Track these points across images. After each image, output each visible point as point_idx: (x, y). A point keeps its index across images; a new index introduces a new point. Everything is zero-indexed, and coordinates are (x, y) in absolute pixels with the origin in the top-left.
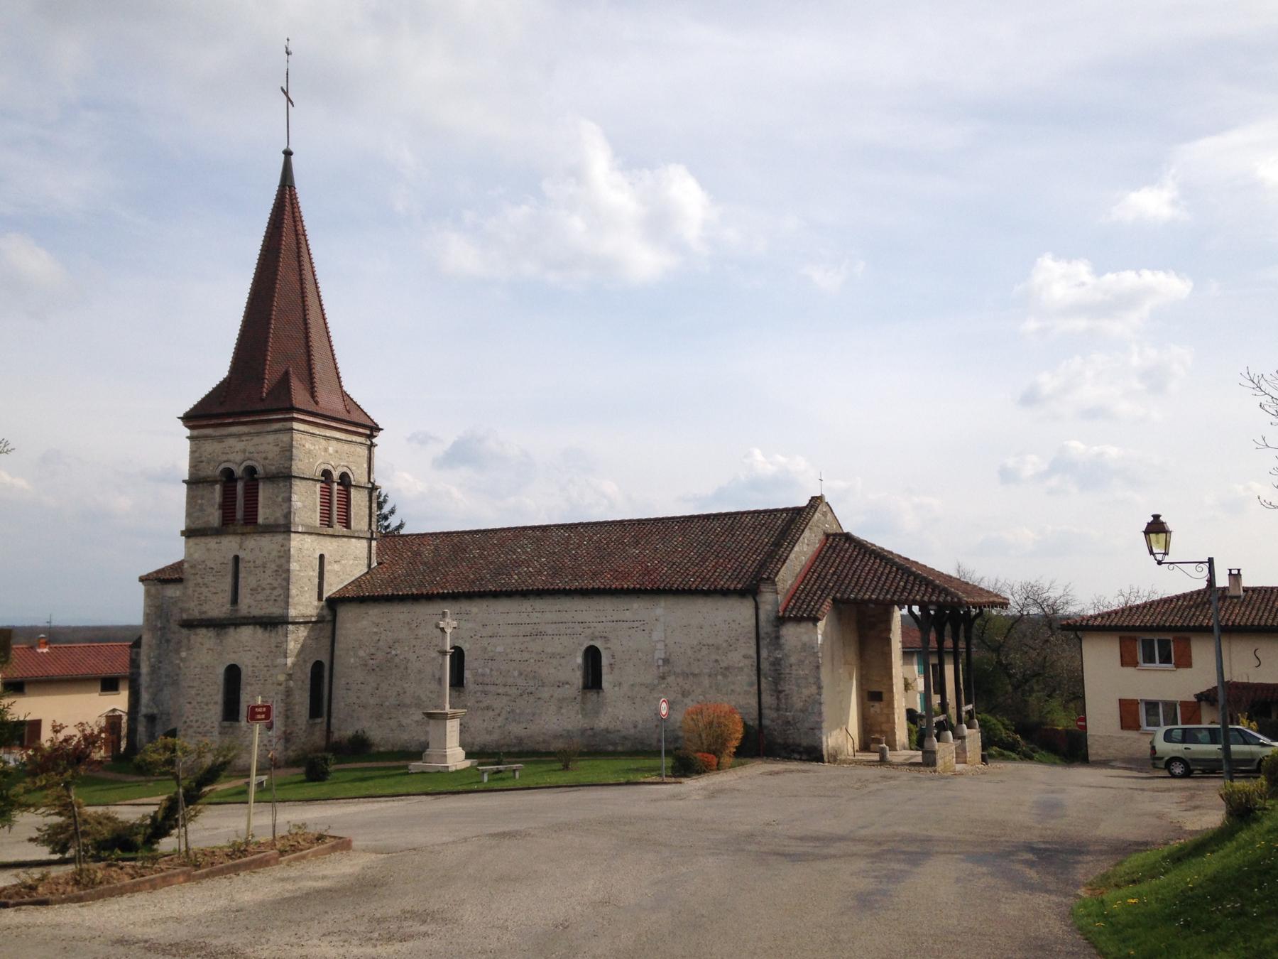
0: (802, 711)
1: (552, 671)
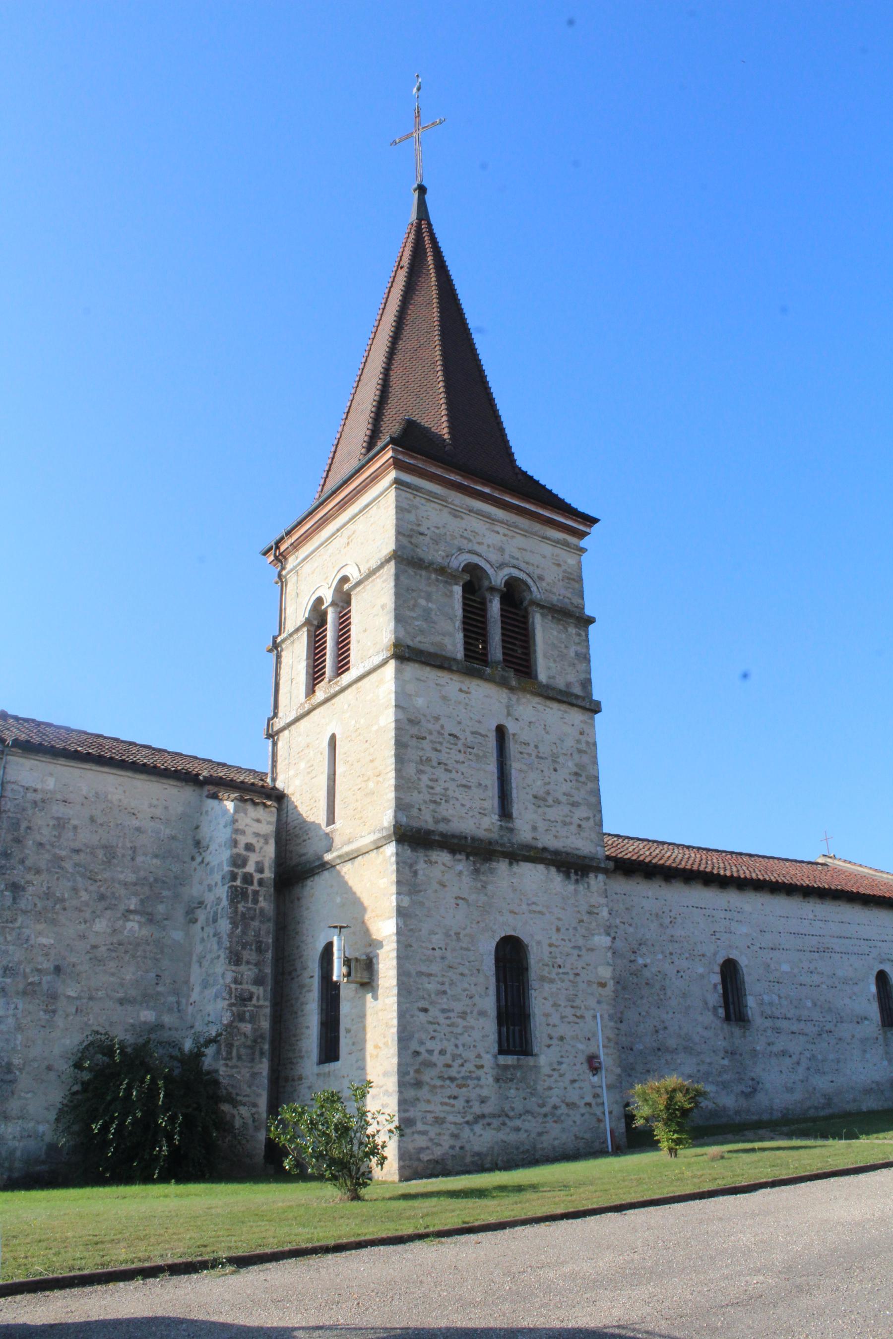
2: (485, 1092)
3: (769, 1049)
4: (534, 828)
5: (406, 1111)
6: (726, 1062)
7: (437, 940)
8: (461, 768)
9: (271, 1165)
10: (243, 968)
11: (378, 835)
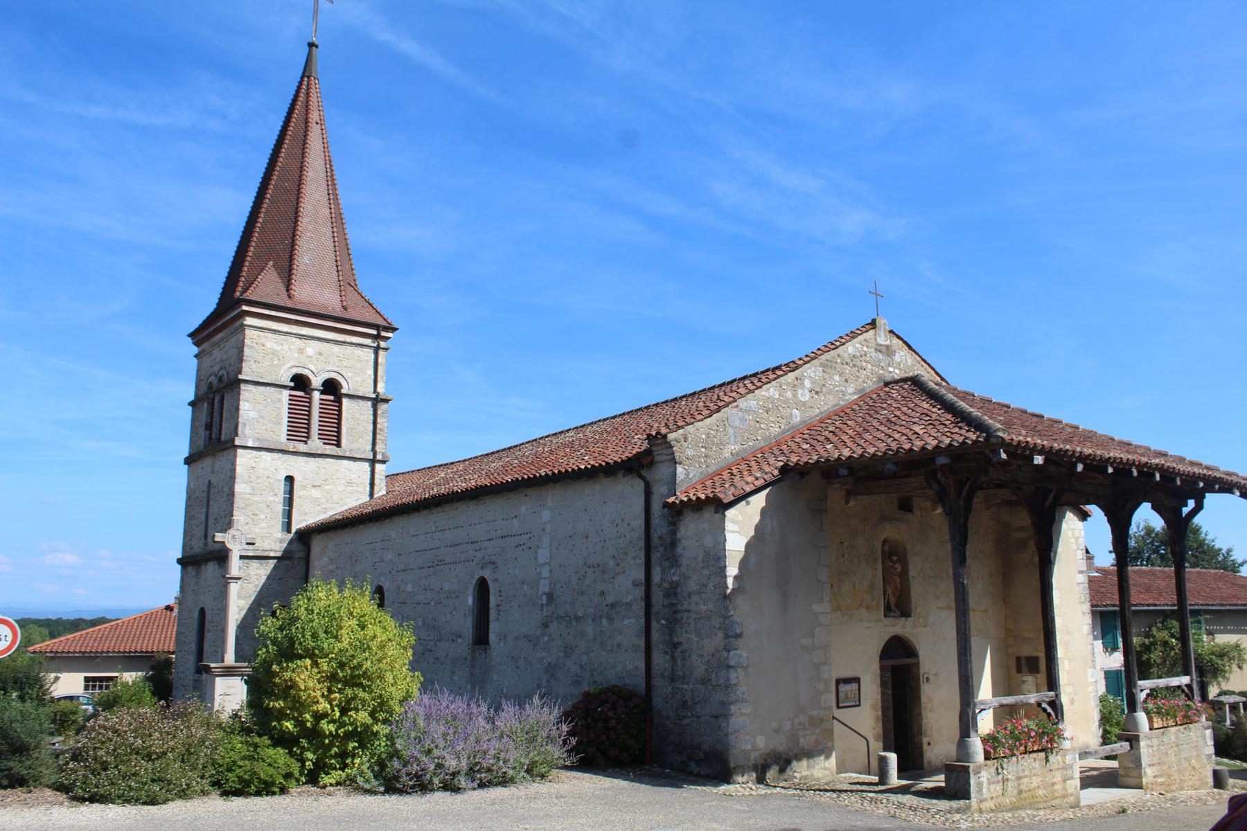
0: (705, 681)
1: (449, 617)
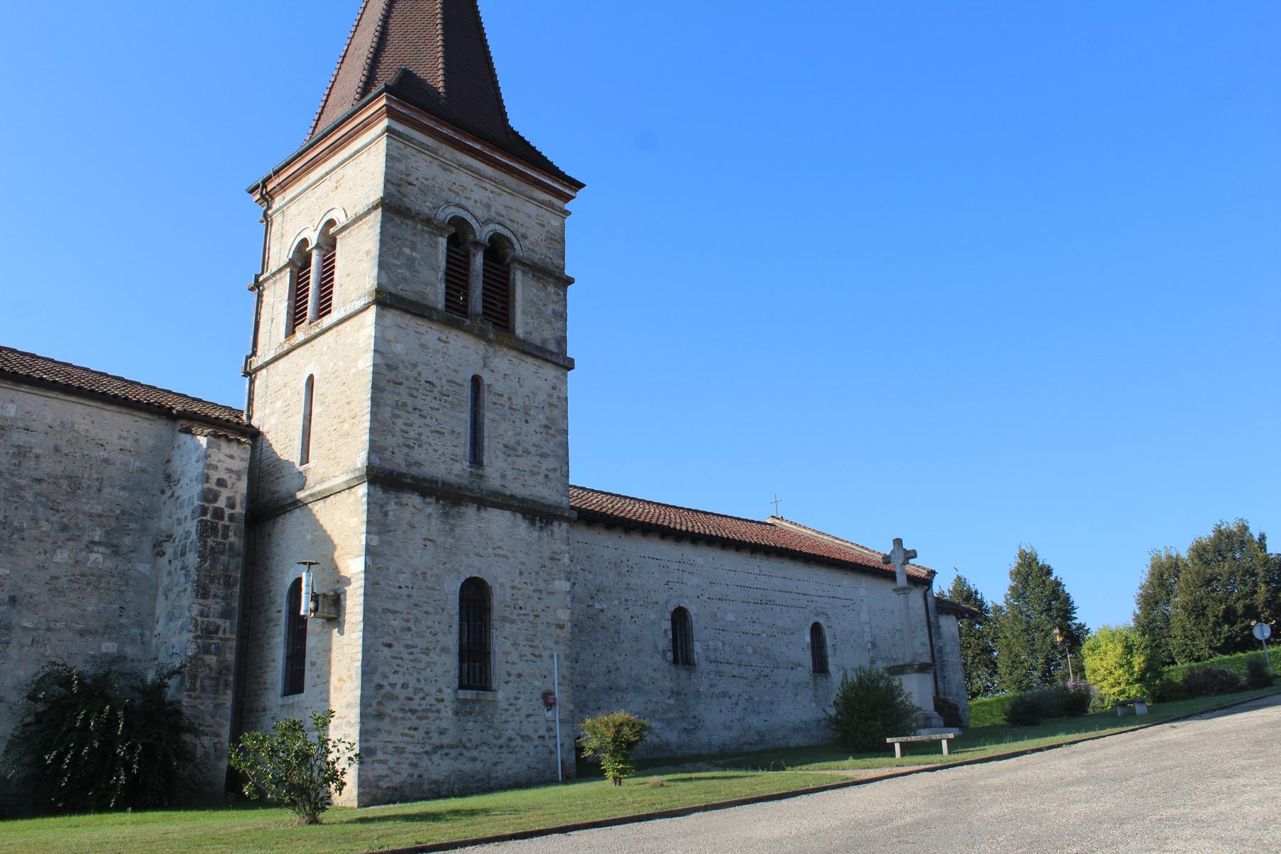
1: (784, 649)
2: (444, 724)
3: (712, 690)
4: (503, 476)
5: (367, 741)
6: (671, 701)
7: (404, 579)
8: (435, 414)
9: (232, 793)
10: (210, 601)
11: (351, 476)
